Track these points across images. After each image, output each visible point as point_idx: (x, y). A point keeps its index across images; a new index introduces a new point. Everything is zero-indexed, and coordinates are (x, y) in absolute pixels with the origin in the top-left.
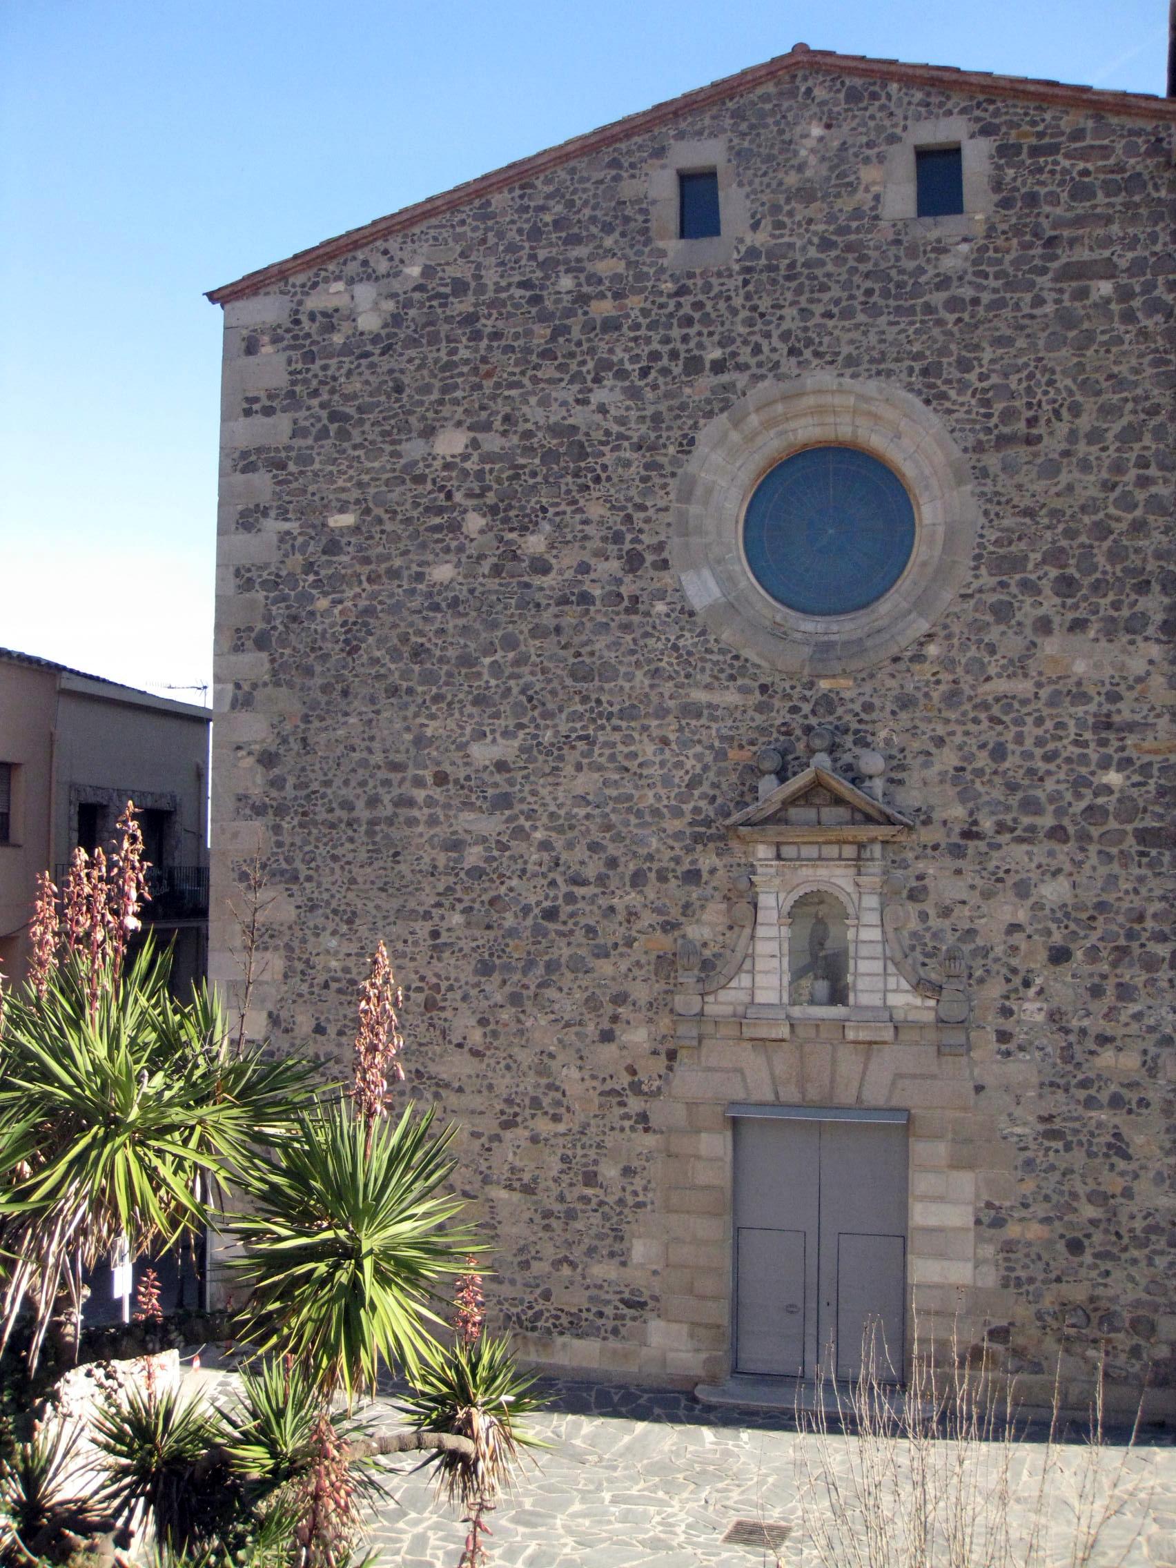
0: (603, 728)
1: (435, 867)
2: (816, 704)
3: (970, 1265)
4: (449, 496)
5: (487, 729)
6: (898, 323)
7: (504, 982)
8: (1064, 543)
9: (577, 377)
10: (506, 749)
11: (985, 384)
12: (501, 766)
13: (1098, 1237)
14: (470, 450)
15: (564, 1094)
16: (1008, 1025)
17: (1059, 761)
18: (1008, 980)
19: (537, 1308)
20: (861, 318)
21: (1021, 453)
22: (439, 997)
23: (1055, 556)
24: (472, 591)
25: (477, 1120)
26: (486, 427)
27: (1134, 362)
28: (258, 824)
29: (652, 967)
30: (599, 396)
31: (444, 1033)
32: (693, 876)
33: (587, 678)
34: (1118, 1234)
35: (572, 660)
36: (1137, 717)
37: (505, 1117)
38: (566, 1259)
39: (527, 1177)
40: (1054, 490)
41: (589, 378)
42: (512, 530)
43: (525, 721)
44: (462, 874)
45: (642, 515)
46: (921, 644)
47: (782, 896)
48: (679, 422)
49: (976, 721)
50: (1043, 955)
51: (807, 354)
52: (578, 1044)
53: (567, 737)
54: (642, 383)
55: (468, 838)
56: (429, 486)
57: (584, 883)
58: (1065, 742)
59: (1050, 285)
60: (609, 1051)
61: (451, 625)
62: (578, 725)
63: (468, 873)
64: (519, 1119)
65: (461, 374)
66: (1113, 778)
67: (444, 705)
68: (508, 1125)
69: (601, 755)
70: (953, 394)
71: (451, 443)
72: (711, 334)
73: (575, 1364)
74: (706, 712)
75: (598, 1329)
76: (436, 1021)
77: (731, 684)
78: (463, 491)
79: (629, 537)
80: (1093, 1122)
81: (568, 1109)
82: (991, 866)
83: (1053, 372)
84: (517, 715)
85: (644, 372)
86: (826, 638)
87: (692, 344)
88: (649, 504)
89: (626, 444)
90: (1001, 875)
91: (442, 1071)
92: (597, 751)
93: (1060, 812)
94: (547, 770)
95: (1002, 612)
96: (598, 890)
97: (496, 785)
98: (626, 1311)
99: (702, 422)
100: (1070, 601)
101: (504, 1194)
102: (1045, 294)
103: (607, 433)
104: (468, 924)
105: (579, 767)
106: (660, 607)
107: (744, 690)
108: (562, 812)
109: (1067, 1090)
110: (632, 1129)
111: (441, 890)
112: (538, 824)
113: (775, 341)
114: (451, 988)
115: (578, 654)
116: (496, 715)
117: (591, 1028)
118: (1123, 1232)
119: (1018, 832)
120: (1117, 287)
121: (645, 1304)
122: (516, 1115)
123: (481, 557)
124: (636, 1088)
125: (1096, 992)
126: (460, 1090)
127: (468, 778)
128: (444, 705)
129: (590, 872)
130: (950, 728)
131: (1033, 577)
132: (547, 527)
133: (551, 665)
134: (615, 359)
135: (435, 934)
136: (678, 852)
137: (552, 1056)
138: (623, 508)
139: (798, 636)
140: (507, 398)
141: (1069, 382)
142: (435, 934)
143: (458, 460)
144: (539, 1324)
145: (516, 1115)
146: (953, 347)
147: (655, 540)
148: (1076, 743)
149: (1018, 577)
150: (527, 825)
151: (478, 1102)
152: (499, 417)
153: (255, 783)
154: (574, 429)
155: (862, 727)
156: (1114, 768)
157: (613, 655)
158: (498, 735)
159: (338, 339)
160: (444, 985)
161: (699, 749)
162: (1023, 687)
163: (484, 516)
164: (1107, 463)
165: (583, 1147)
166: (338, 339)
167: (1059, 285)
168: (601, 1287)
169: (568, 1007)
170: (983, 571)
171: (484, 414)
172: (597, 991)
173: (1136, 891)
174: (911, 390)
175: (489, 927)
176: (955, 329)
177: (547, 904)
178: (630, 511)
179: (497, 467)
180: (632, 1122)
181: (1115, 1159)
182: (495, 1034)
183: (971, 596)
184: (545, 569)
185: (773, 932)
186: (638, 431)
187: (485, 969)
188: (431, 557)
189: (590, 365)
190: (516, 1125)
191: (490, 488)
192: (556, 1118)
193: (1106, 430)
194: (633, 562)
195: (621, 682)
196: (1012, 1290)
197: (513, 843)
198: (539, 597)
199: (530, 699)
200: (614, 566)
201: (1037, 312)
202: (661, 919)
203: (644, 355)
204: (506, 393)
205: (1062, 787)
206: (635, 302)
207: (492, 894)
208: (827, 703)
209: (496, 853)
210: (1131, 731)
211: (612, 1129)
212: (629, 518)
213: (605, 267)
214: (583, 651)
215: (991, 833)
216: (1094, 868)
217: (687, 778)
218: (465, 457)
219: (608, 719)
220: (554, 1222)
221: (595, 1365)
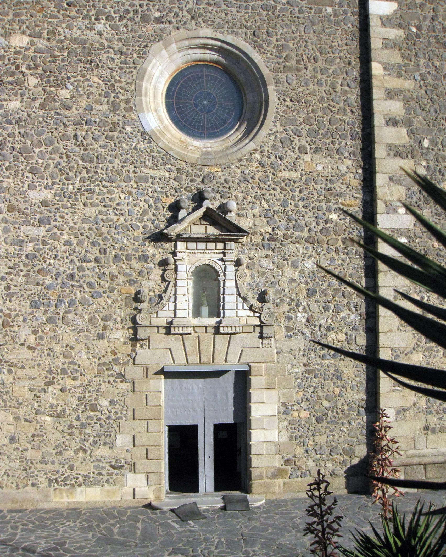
0: (99, 185)
1: (8, 254)
2: (204, 177)
3: (277, 432)
4: (18, 67)
5: (37, 184)
6: (241, 12)
7: (46, 311)
8: (312, 115)
9: (86, 17)
10: (47, 194)
11: (278, 43)
12: (44, 203)
13: (330, 414)
14: (30, 46)
15: (79, 366)
16: (290, 324)
17: (310, 208)
18: (290, 304)
19: (66, 475)
20: (224, 7)
22: (10, 320)
24: (29, 115)
25: (33, 382)
26: (39, 36)
27: (340, 42)
29: (123, 302)
30: (99, 27)
31: (13, 339)
32: (144, 258)
33: (91, 161)
34: (337, 413)
35: (82, 152)
36: (342, 191)
37: (47, 380)
38: (81, 448)
39: (59, 409)
40: (308, 92)
41: (93, 18)
42: (50, 87)
43: (57, 181)
44: (23, 257)
45: (119, 85)
46: (251, 154)
47: (188, 267)
48: (138, 43)
49: (274, 189)
50: (305, 292)
51: (200, 20)
52: (85, 342)
53: (80, 189)
54: (120, 23)
55: (26, 239)
56: (7, 62)
57: (89, 261)
58: (314, 200)
59: (304, 5)
60: (102, 344)
61: (17, 132)
62: (86, 184)
63: (27, 256)
64: (55, 380)
65: (26, 8)
67: (13, 172)
68: (49, 384)
69: (97, 199)
70: (265, 46)
72: (154, 5)
73: (88, 499)
74: (150, 180)
75: (99, 481)
76: (9, 332)
77: (162, 167)
78: (25, 66)
79: (113, 95)
80: (326, 365)
81: (81, 374)
82: (282, 253)
83: (306, 42)
84: (52, 178)
85: (121, 19)
86: (205, 149)
87: (145, 8)
88: (123, 80)
89: (112, 51)
90: (287, 257)
91: (12, 357)
92: (95, 197)
93: (309, 231)
94: (69, 205)
96: (96, 265)
97: (41, 213)
98: (113, 471)
99: (149, 45)
100: (314, 139)
101: (48, 419)
102: (304, 9)
103: (102, 44)
104: (27, 283)
105: (85, 205)
106: (128, 129)
107: (170, 171)
108: (77, 227)
109: (315, 352)
110: (114, 381)
111: (11, 265)
112: (64, 232)
113: (185, 13)
114: (17, 315)
115: (85, 150)
116: (42, 178)
117: (93, 331)
118: (339, 412)
119: (293, 239)
120: (334, 11)
121: (123, 466)
122: (54, 378)
123: (35, 99)
124: (116, 361)
125: (326, 309)
126: (23, 367)
127: (26, 209)
128: (13, 172)
129: (91, 256)
130: (263, 192)
131: (299, 128)
132: (71, 87)
133: (71, 154)
134: (107, 11)
135: (8, 288)
136: (137, 246)
137: (72, 347)
138: (109, 81)
139: (193, 148)
140: (50, 22)
141: (314, 47)
142: (8, 288)
143: (23, 50)
144: (68, 483)
145: (54, 378)
146: (265, 25)
147: (125, 98)
148: (318, 201)
149: (293, 127)
150: (58, 232)
151: (32, 373)
152: (46, 32)
154: (85, 41)
155: (225, 190)
156: (333, 211)
157: (103, 150)
158: (43, 188)
160: (13, 314)
161: (147, 197)
162: (295, 175)
163: (37, 78)
164: (329, 83)
165: (89, 392)
167: (310, 6)
168: (99, 461)
169: (81, 323)
170: (278, 124)
171: (37, 29)
172: (96, 315)
173: (342, 265)
174: (247, 42)
175: (38, 284)
176: (266, 19)
177: (69, 272)
178: (113, 82)
179: (44, 55)
180: (114, 378)
181: (335, 380)
182: (41, 338)
183: (273, 134)
184: (68, 108)
185: (184, 283)
186: (118, 46)
187: (35, 305)
188: (7, 97)
189: (94, 12)
190: (54, 383)
191: (39, 65)
192: (74, 379)
193: (329, 69)
194: (114, 107)
195: (107, 164)
196: (294, 442)
197: (51, 241)
198: (65, 120)
199: (60, 170)
200: (105, 108)
201: (300, 16)
202: (128, 279)
203: (122, 10)
204: (50, 20)
205: (311, 220)
207: (40, 267)
209: (41, 247)
210: (340, 196)
211: (104, 382)
212: (113, 86)
214: (89, 148)
215: (281, 239)
216: (325, 255)
217: (141, 211)
218: (27, 49)
219: (101, 182)
220: (74, 430)
221: (98, 499)
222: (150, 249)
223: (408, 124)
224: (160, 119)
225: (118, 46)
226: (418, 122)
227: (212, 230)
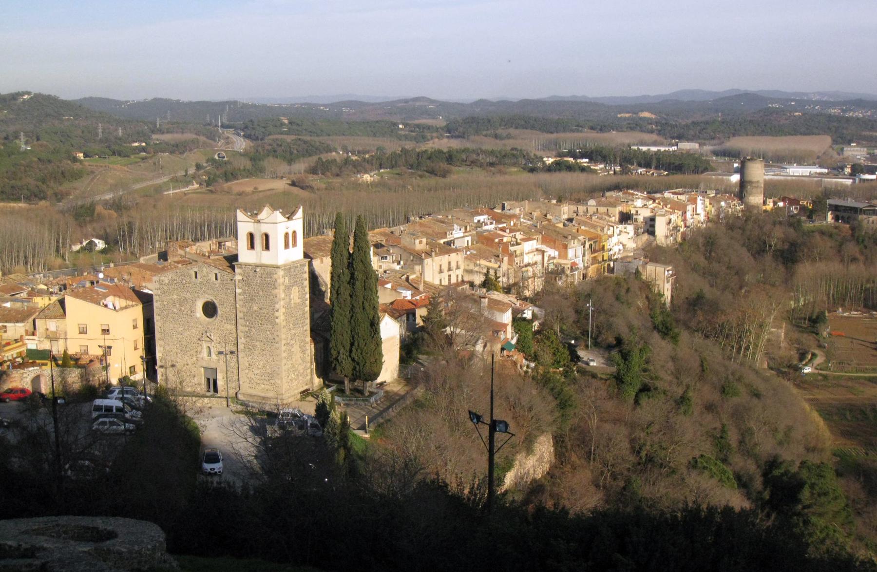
10: (182, 329)
66: (231, 338)
71: (175, 296)
166: (164, 283)
169: (189, 355)
194: (191, 312)
200: (190, 312)
206: (190, 285)
222: (199, 342)
227: (209, 339)
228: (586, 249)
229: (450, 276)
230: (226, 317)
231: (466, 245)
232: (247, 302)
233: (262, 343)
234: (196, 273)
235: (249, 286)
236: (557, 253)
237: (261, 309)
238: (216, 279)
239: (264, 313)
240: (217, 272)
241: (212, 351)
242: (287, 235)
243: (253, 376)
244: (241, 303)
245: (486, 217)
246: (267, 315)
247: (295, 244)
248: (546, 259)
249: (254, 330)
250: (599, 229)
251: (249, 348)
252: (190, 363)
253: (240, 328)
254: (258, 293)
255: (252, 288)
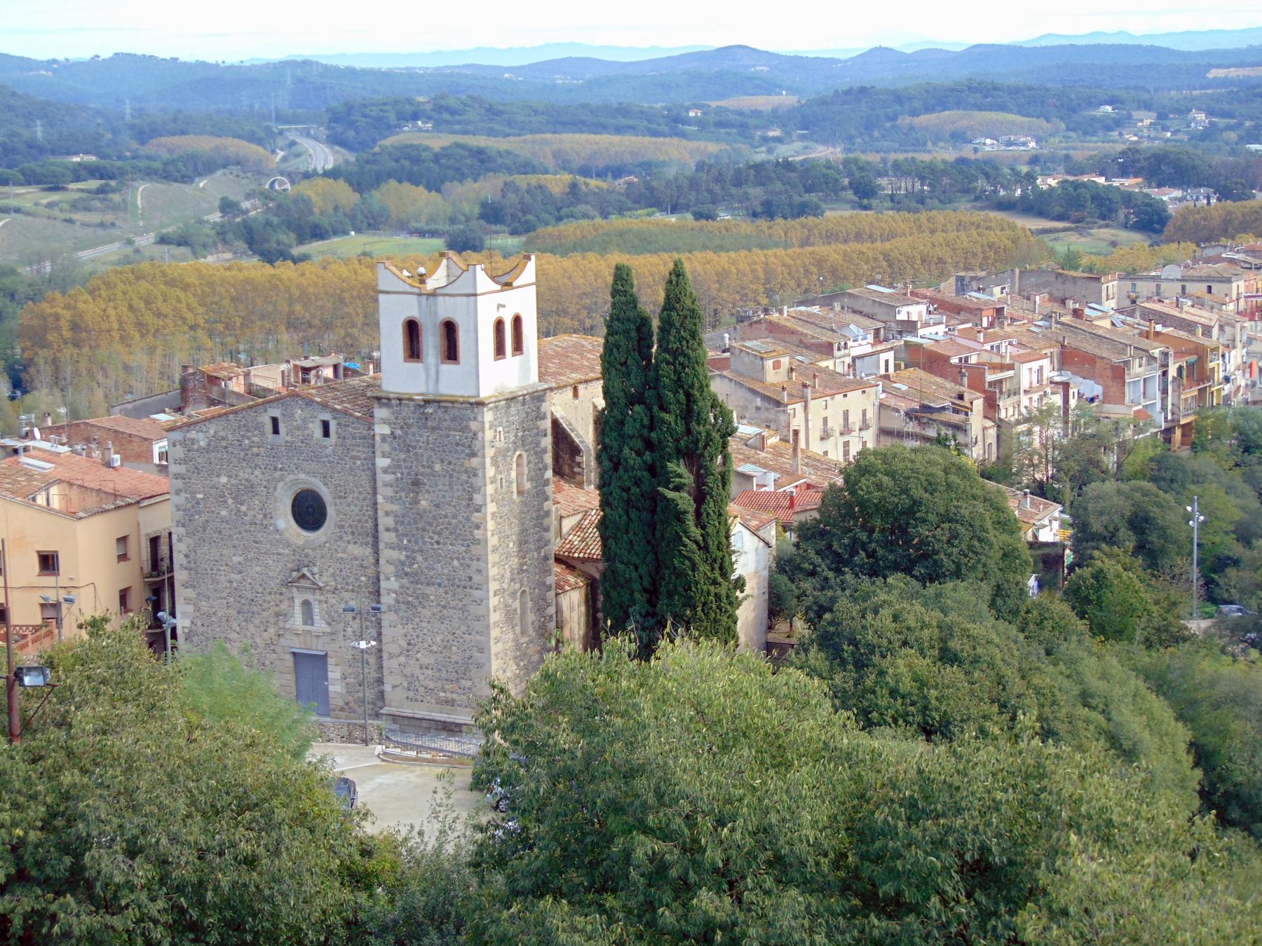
10: (240, 559)
21: (343, 501)
23: (350, 526)
28: (186, 572)
32: (281, 594)
66: (363, 579)
95: (341, 538)
153: (185, 562)
159: (195, 447)
166: (195, 447)
169: (257, 622)
186: (264, 483)
187: (239, 612)
194: (265, 516)
200: (260, 517)
208: (307, 556)
213: (256, 439)
223: (396, 530)
224: (288, 521)
225: (264, 483)
226: (401, 528)
228: (1170, 379)
229: (846, 444)
230: (350, 526)
231: (882, 372)
232: (403, 490)
233: (441, 590)
234: (275, 421)
235: (408, 451)
236: (1098, 390)
237: (437, 506)
238: (326, 433)
239: (446, 516)
240: (327, 416)
241: (316, 610)
242: (499, 325)
243: (418, 672)
244: (389, 492)
245: (923, 308)
246: (454, 521)
247: (518, 347)
248: (1073, 403)
249: (419, 558)
250: (1200, 331)
251: (408, 603)
252: (258, 640)
253: (386, 554)
254: (429, 467)
255: (416, 454)
